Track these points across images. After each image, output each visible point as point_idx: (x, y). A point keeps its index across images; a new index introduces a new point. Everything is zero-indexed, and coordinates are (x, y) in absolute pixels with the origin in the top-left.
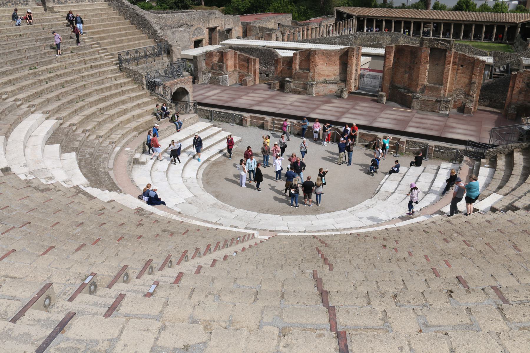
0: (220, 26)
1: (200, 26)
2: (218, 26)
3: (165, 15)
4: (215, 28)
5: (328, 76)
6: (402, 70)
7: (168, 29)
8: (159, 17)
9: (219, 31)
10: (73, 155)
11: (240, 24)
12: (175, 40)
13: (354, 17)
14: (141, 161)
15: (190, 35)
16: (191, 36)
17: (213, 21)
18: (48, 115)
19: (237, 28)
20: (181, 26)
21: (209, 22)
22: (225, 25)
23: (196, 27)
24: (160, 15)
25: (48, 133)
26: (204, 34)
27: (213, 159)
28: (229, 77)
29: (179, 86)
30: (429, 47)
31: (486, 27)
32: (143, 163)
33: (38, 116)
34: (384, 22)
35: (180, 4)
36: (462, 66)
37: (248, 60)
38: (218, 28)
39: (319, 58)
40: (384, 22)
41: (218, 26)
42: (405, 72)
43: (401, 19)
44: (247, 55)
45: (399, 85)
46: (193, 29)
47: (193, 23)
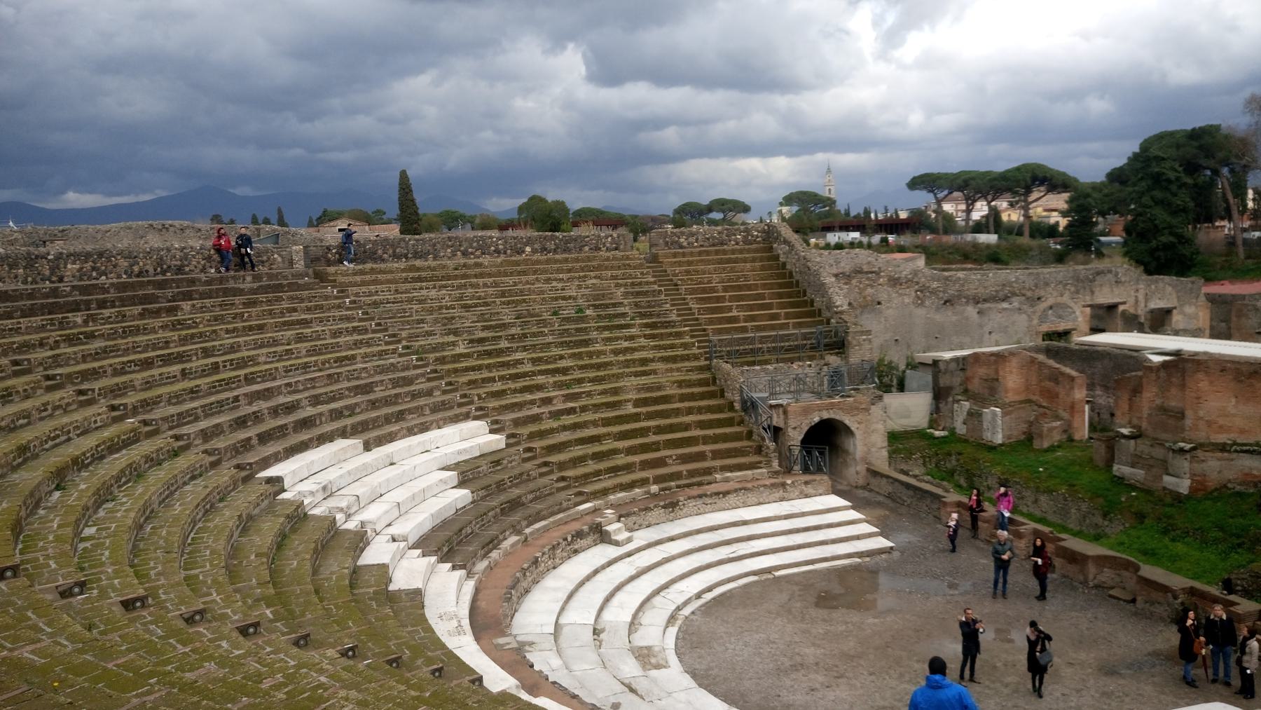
0: (1131, 301)
1: (1066, 299)
2: (1124, 303)
3: (961, 274)
4: (1112, 308)
5: (1242, 431)
7: (967, 303)
8: (947, 278)
9: (1124, 312)
10: (462, 496)
11: (1202, 298)
12: (987, 329)
14: (614, 537)
15: (1030, 320)
16: (1035, 322)
17: (1106, 289)
18: (495, 427)
19: (1189, 310)
21: (1093, 292)
22: (1147, 301)
23: (1051, 301)
24: (946, 274)
25: (460, 452)
26: (1075, 319)
27: (778, 574)
28: (1004, 414)
29: (826, 415)
32: (617, 544)
33: (481, 425)
35: (1161, 254)
37: (1056, 377)
38: (1121, 308)
39: (1211, 382)
41: (1124, 303)
44: (1058, 366)
46: (1043, 306)
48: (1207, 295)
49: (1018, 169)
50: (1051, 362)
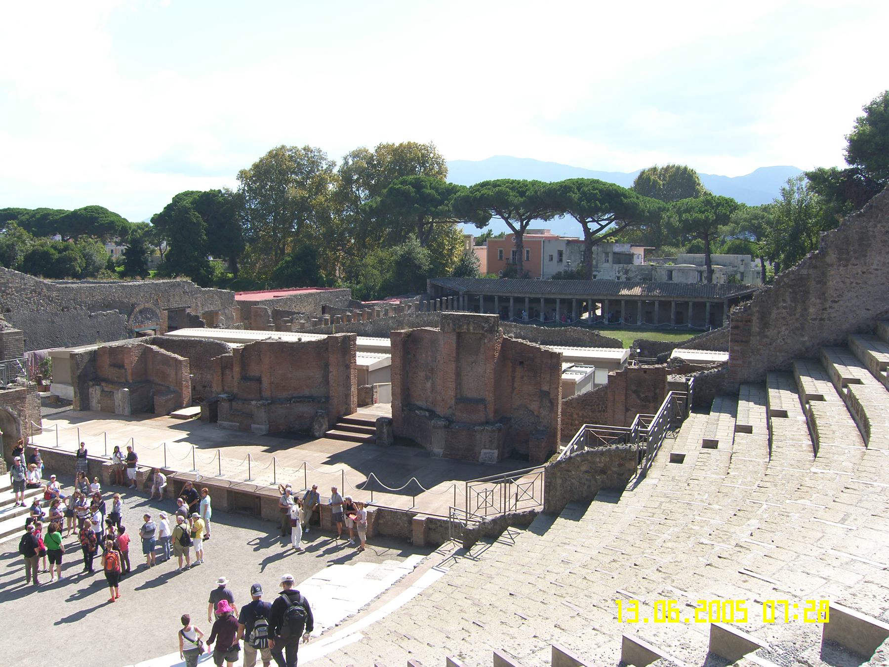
4: (183, 310)
6: (422, 374)
13: (461, 293)
17: (177, 298)
20: (108, 306)
23: (142, 307)
30: (454, 330)
31: (676, 304)
34: (512, 301)
36: (521, 363)
38: (188, 311)
40: (512, 301)
42: (427, 378)
43: (540, 296)
45: (419, 403)
47: (133, 300)
48: (239, 302)
49: (86, 209)
50: (163, 351)
